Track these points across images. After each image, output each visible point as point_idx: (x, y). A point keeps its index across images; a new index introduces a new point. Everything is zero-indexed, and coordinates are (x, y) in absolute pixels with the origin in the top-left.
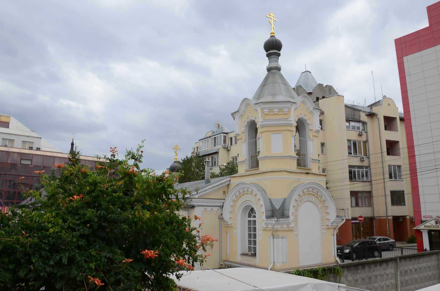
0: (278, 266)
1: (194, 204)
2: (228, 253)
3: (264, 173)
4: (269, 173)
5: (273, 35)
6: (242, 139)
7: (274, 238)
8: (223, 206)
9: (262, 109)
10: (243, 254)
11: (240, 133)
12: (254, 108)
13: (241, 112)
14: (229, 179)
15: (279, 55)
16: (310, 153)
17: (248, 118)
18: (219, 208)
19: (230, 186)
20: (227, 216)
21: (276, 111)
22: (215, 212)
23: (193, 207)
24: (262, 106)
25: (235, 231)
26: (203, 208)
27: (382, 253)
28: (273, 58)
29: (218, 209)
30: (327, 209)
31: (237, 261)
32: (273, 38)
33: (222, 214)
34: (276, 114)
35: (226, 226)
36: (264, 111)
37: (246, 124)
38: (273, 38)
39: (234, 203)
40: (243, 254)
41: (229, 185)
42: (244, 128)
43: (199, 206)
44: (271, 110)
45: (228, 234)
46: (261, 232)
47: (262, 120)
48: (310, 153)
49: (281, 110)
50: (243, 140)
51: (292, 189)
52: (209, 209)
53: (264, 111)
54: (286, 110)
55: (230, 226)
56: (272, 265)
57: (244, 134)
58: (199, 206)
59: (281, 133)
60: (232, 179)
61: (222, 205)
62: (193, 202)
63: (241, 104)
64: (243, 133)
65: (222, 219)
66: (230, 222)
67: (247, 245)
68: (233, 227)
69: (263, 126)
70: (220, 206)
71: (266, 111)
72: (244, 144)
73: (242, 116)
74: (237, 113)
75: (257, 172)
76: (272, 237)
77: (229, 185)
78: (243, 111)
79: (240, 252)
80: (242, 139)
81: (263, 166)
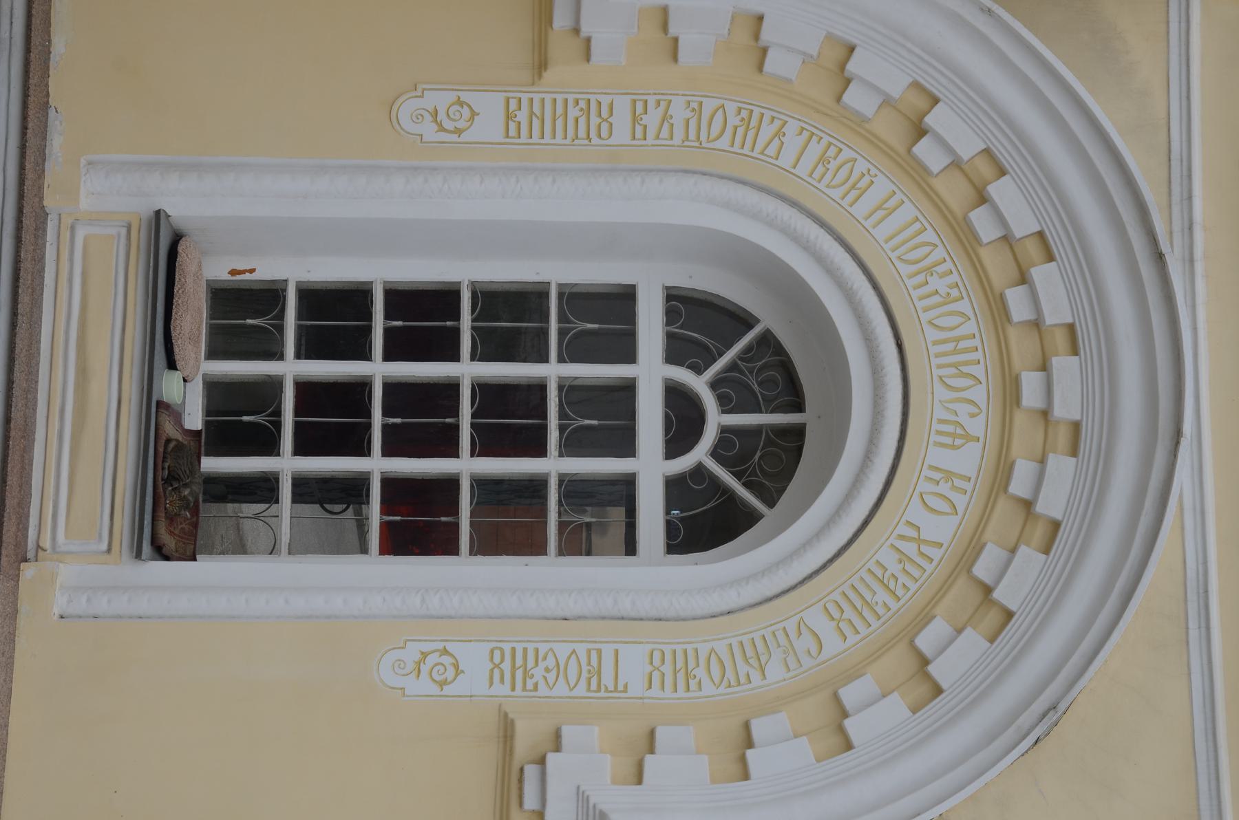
10: (166, 249)
25: (490, 106)
31: (57, 143)
39: (887, 102)
40: (166, 249)
46: (475, 675)
67: (294, 269)
68: (541, 65)
79: (184, 203)
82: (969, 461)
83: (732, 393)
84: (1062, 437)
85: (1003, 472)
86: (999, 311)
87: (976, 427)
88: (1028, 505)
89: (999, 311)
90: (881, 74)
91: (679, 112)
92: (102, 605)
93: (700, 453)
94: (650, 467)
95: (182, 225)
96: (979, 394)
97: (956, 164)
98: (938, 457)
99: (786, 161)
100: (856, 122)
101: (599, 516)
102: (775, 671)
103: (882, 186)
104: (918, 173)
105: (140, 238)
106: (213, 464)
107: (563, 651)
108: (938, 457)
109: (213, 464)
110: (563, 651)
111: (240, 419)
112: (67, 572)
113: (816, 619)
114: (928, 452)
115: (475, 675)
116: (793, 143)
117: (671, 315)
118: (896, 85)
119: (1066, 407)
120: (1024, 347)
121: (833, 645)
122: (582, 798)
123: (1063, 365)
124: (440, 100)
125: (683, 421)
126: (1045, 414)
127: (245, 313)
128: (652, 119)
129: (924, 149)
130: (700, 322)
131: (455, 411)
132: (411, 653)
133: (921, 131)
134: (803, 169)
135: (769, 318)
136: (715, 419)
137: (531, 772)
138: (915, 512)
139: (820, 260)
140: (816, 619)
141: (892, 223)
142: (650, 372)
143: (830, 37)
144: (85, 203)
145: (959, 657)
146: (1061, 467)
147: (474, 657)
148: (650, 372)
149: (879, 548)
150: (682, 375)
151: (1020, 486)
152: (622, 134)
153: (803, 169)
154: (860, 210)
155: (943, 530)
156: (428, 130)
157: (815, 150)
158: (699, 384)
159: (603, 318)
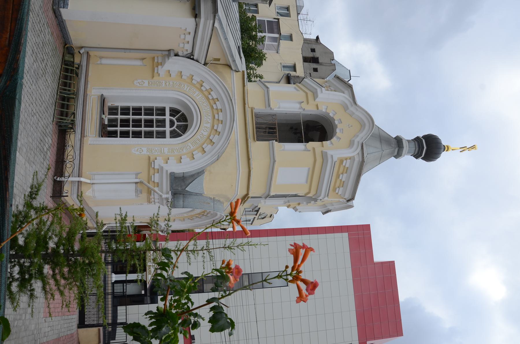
0: (87, 194)
1: (202, 20)
2: (104, 61)
3: (249, 159)
4: (247, 170)
5: (446, 149)
6: (308, 103)
7: (136, 183)
8: (193, 59)
9: (352, 159)
10: (103, 100)
11: (317, 100)
12: (357, 140)
13: (352, 109)
14: (241, 70)
15: (417, 156)
16: (265, 202)
17: (340, 121)
18: (190, 51)
19: (227, 70)
20: (174, 65)
21: (344, 177)
22: (182, 45)
23: (196, 15)
24: (358, 159)
25: (146, 82)
26: (192, 30)
27: (119, 321)
28: (414, 148)
29: (187, 50)
30: (180, 220)
31: (89, 86)
32: (442, 150)
33: (176, 55)
34: (338, 176)
35: (153, 59)
36: (348, 161)
37: (331, 115)
38: (442, 150)
39: (198, 82)
40: (103, 100)
41: (230, 66)
42: (324, 110)
43: (197, 25)
44: (347, 170)
45: (139, 63)
46: (145, 151)
47: (335, 159)
48: (265, 202)
49: (343, 184)
50: (304, 105)
51: (217, 198)
52: (190, 38)
53: (348, 161)
54: (341, 191)
55: (156, 71)
56: (89, 181)
57: (315, 109)
58: (197, 25)
59: (307, 182)
60: (240, 75)
61: (195, 58)
62: (206, 19)
63: (366, 112)
64: (317, 106)
65: (169, 56)
66: (162, 70)
67: (120, 104)
68: (153, 77)
69: (324, 156)
70: (192, 54)
71: (348, 164)
72: (298, 106)
73: (345, 108)
74: (351, 101)
75: (250, 140)
76: (137, 180)
77: (230, 66)
78: (354, 113)
79: (106, 93)
80: (308, 103)
81: (260, 148)
82: (209, 125)
83: (178, 120)
84: (220, 122)
85: (213, 126)
86: (212, 107)
87: (210, 121)
88: (216, 130)
89: (212, 107)
90: (197, 79)
91: (171, 83)
92: (95, 143)
93: (174, 127)
94: (168, 129)
95: (105, 96)
96: (210, 117)
97: (206, 90)
98: (205, 125)
99: (185, 89)
100: (194, 85)
101: (162, 135)
102: (184, 151)
103: (197, 93)
104: (202, 91)
105: (100, 98)
106: (108, 128)
107: (156, 148)
108: (205, 125)
109: (110, 129)
110: (156, 148)
111: (113, 123)
112: (90, 139)
113: (190, 144)
114: (204, 125)
115: (145, 151)
116: (186, 87)
117: (170, 111)
118: (199, 80)
119: (221, 119)
120: (215, 111)
121: (192, 147)
122: (159, 165)
123: (220, 113)
124: (140, 81)
125: (172, 123)
126: (218, 120)
127: (113, 110)
128: (168, 84)
129: (202, 88)
130: (174, 112)
131: (141, 122)
132: (136, 149)
133: (202, 86)
134: (187, 90)
135: (183, 111)
136: (176, 123)
137: (153, 163)
138: (202, 132)
139: (190, 101)
140: (190, 144)
141: (199, 97)
142: (168, 117)
143: (190, 74)
144: (93, 93)
145: (208, 148)
146: (220, 125)
147: (145, 149)
148: (168, 117)
149: (198, 136)
150: (172, 118)
151: (215, 128)
152: (164, 85)
153: (187, 90)
154: (195, 95)
155: (206, 134)
156: (138, 84)
157: (189, 88)
158: (174, 119)
159: (161, 111)
